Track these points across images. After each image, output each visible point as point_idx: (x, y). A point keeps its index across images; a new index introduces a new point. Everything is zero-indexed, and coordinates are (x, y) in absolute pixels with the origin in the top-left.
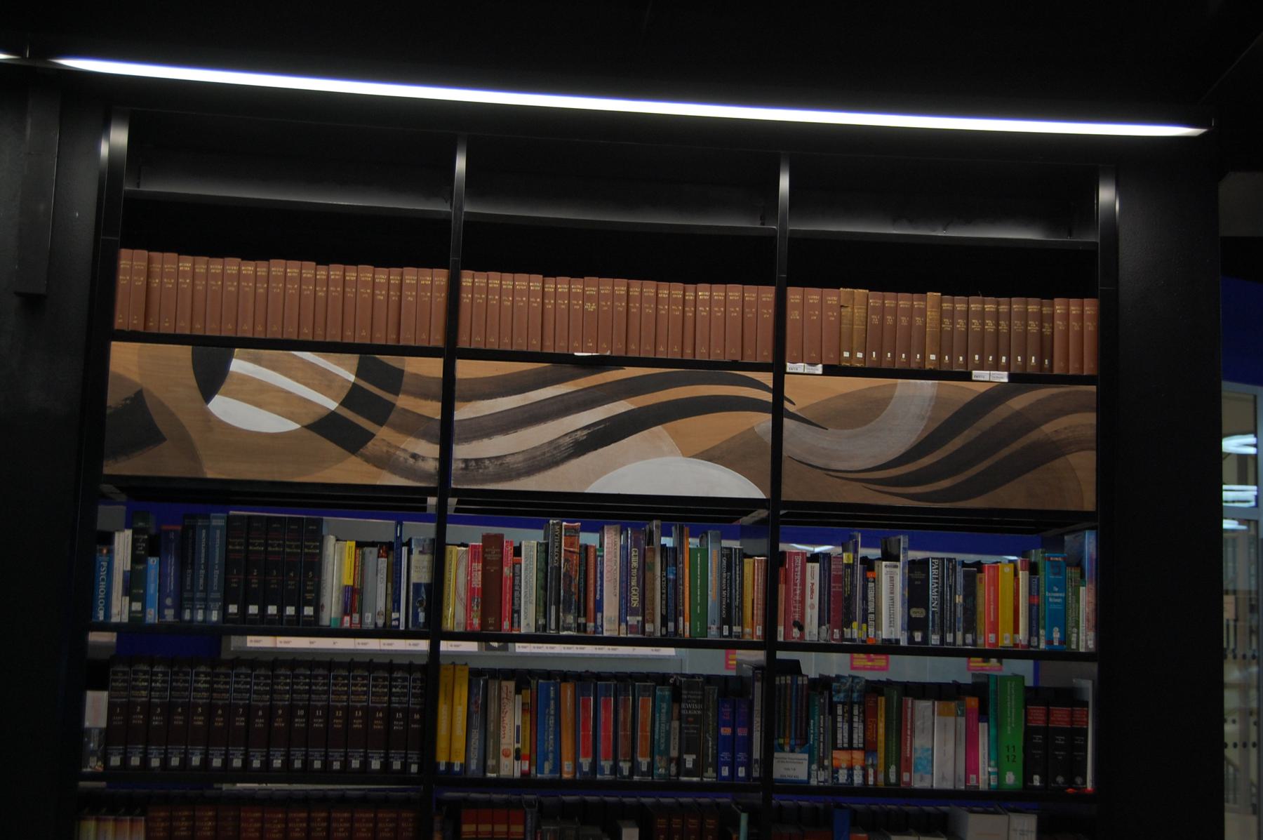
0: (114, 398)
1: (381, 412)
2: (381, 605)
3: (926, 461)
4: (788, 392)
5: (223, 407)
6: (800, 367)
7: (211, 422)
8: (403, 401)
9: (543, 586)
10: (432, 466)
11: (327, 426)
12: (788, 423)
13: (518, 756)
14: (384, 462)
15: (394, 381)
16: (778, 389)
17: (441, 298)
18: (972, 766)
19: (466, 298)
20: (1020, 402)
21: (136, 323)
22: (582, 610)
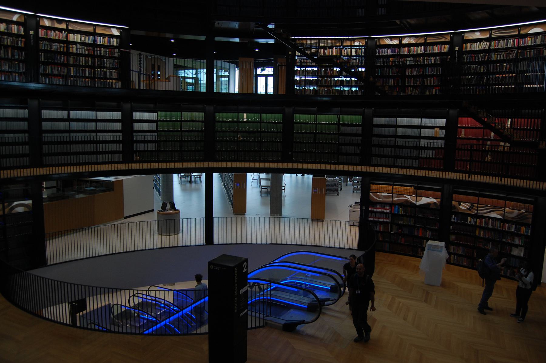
0: (453, 205)
1: (472, 208)
2: (472, 222)
4: (505, 210)
5: (460, 207)
6: (507, 208)
9: (485, 223)
10: (476, 213)
11: (468, 209)
12: (505, 213)
13: (482, 235)
14: (473, 212)
15: (473, 206)
16: (504, 210)
17: (477, 199)
18: (520, 243)
19: (479, 200)
20: (525, 214)
21: (454, 200)
22: (488, 225)
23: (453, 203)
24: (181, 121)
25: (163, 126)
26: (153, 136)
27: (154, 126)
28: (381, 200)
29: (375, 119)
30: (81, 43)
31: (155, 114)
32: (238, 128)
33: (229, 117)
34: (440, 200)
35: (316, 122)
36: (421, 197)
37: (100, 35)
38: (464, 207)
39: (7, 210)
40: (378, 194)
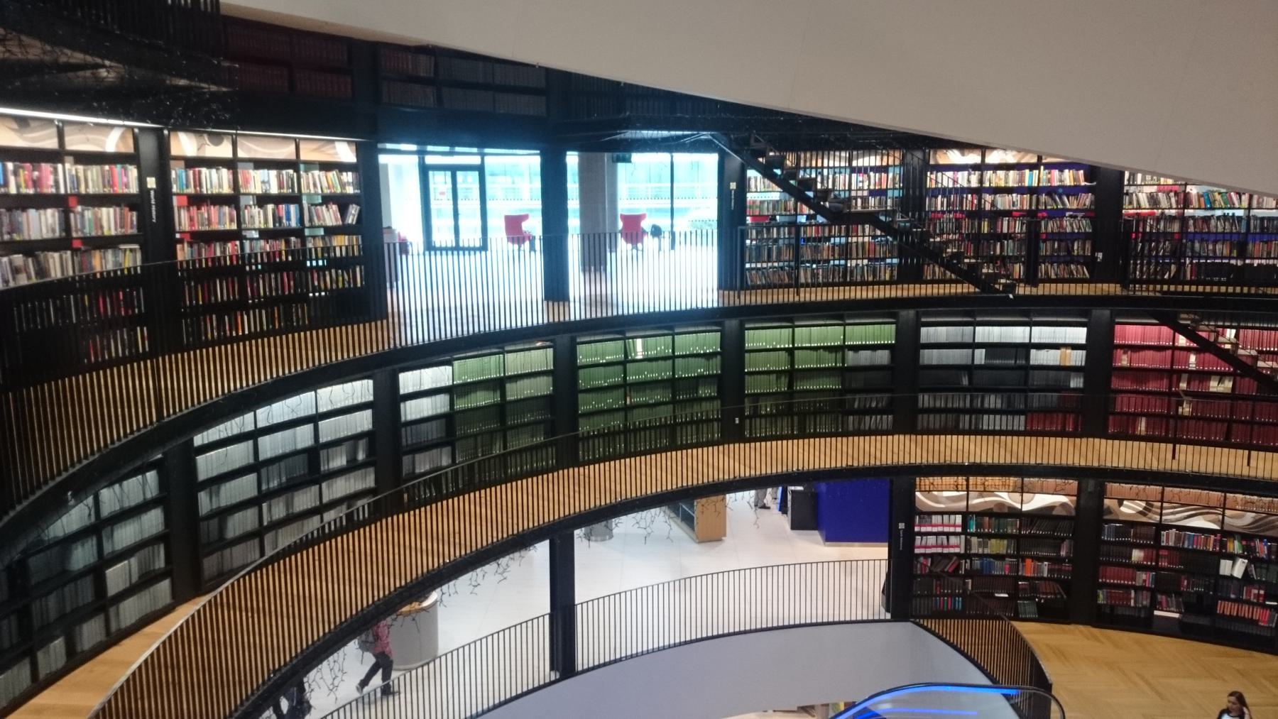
0: (1105, 507)
1: (1150, 511)
3: (1259, 524)
5: (1122, 509)
7: (1121, 512)
8: (1154, 509)
11: (1140, 512)
14: (1150, 518)
15: (1152, 506)
23: (1107, 502)
28: (942, 506)
29: (924, 330)
31: (447, 370)
32: (625, 378)
34: (1075, 498)
35: (793, 344)
36: (1032, 495)
37: (310, 165)
38: (1129, 509)
40: (935, 493)
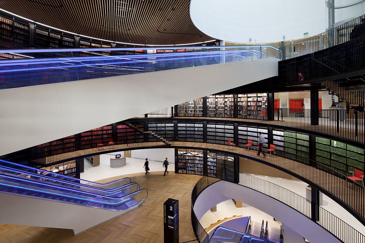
24: (297, 139)
25: (287, 139)
26: (282, 144)
27: (283, 139)
30: (252, 101)
31: (283, 133)
33: (325, 141)
39: (226, 159)
